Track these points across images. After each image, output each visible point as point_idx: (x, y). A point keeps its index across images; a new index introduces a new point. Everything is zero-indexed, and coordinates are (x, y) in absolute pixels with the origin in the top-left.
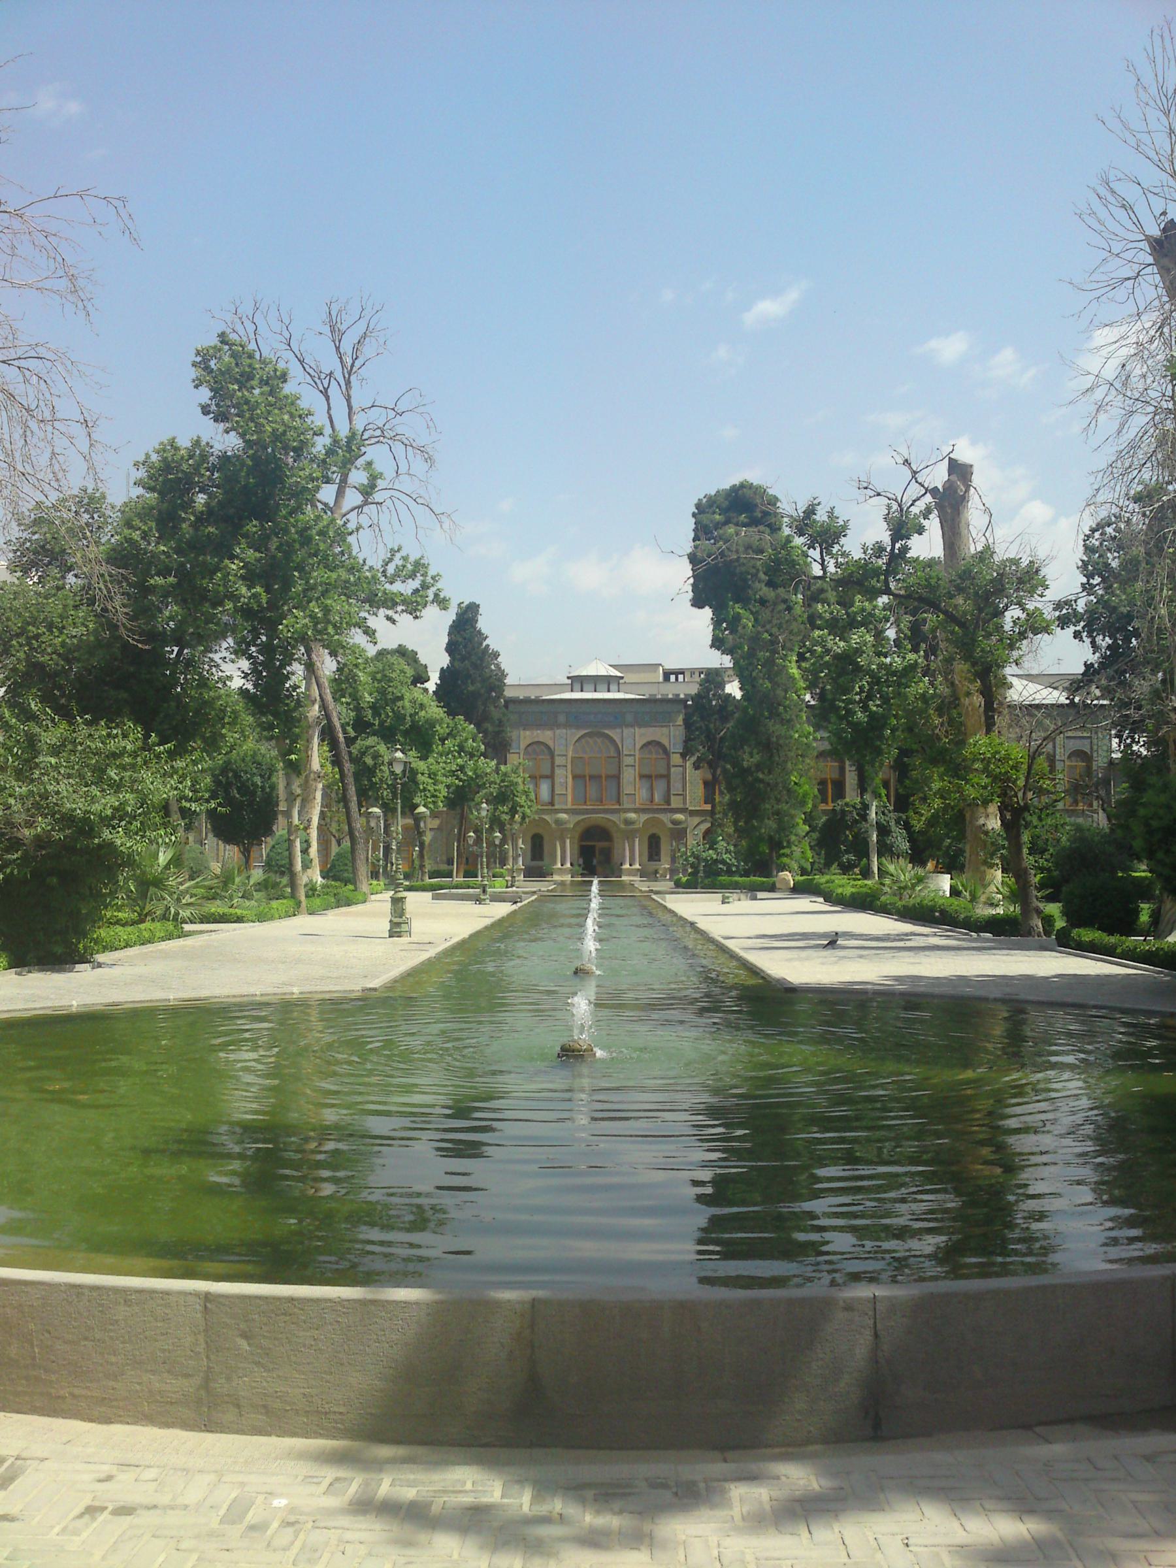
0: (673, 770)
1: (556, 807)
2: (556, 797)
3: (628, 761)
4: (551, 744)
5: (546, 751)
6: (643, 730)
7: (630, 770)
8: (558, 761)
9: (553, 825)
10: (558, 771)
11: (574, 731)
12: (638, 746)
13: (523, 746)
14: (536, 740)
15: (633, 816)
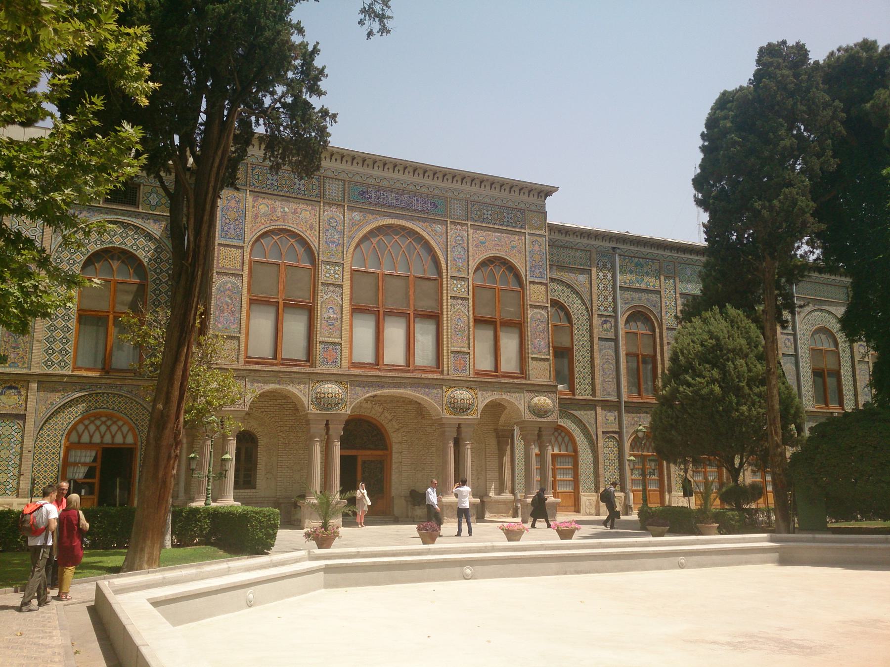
0: (531, 313)
1: (318, 370)
2: (319, 348)
3: (453, 288)
4: (312, 238)
5: (300, 250)
6: (481, 235)
7: (460, 306)
8: (325, 273)
9: (312, 409)
10: (324, 296)
11: (356, 216)
12: (473, 264)
13: (250, 236)
14: (280, 225)
15: (462, 394)
